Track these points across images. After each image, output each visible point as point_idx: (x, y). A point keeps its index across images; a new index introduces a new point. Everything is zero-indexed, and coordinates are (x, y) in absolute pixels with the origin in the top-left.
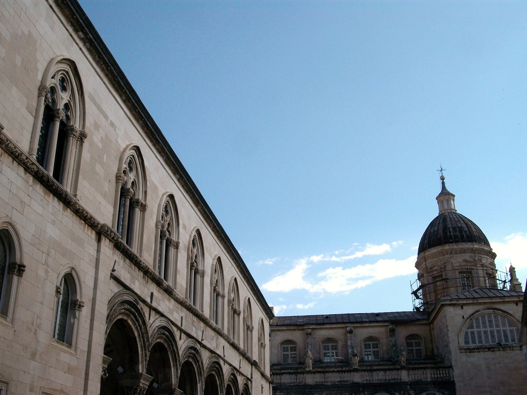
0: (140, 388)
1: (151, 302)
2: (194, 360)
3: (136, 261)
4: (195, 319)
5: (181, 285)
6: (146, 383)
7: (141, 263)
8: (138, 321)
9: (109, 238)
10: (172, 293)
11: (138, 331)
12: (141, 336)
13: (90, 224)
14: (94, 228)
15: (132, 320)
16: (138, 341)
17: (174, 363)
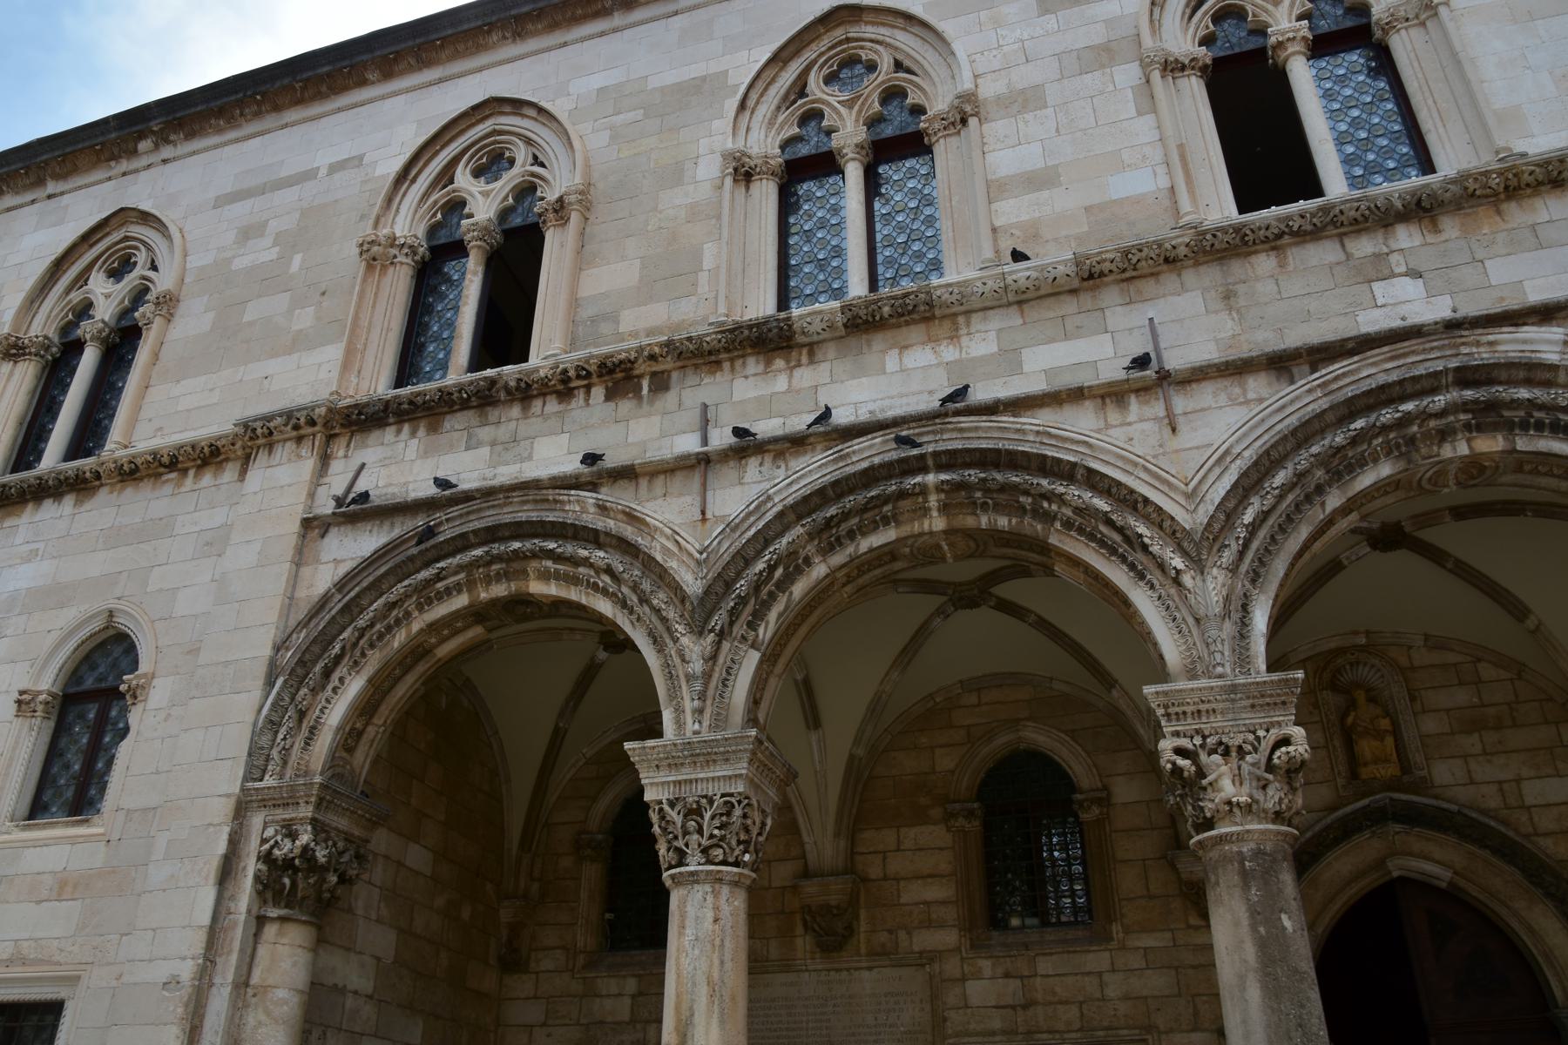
0: (657, 808)
1: (705, 442)
2: (1524, 426)
3: (506, 387)
4: (1406, 237)
5: (1088, 209)
6: (701, 775)
7: (535, 376)
8: (586, 562)
9: (286, 436)
10: (930, 304)
11: (605, 592)
12: (633, 599)
13: (199, 462)
14: (222, 457)
15: (545, 576)
16: (628, 628)
17: (1132, 567)
